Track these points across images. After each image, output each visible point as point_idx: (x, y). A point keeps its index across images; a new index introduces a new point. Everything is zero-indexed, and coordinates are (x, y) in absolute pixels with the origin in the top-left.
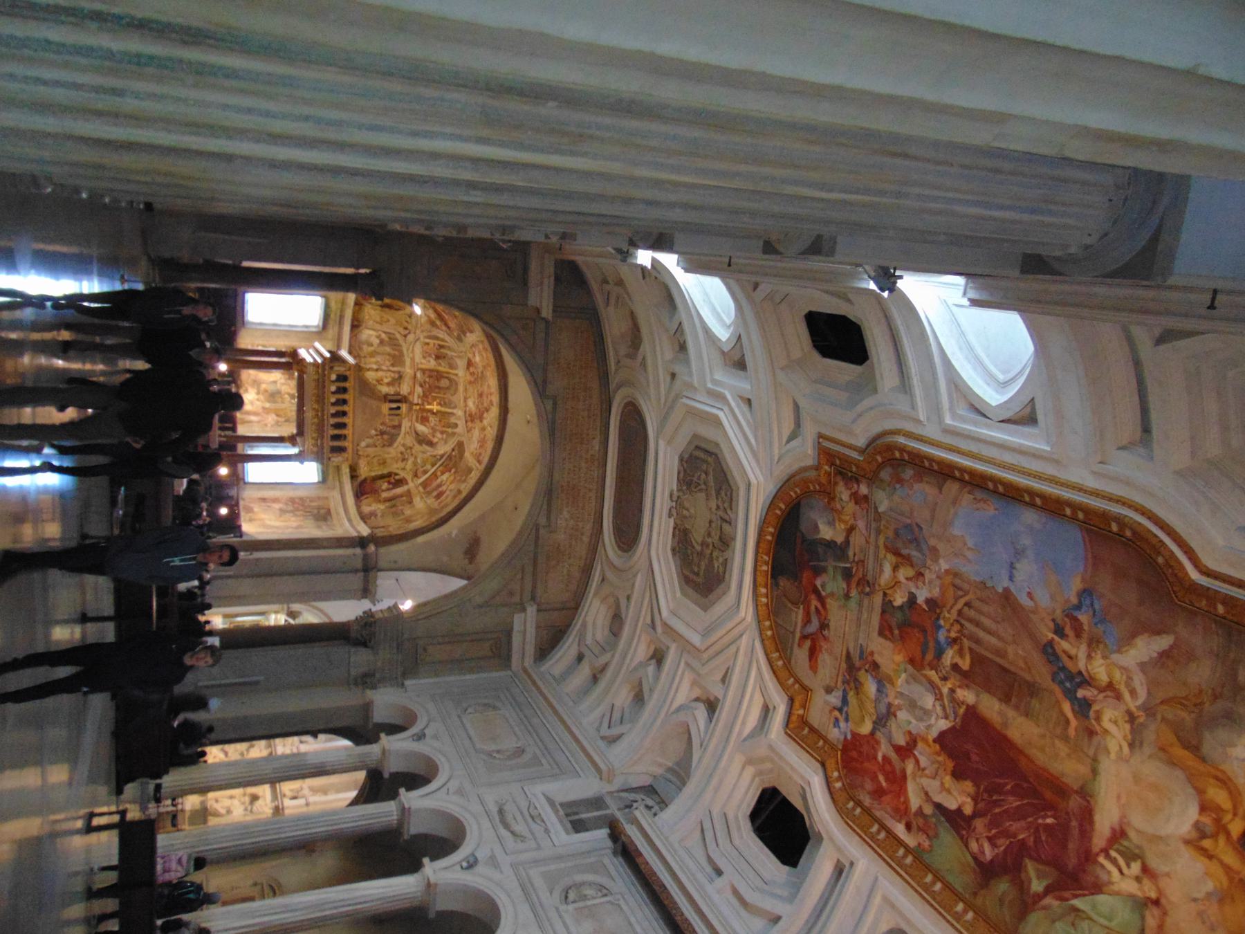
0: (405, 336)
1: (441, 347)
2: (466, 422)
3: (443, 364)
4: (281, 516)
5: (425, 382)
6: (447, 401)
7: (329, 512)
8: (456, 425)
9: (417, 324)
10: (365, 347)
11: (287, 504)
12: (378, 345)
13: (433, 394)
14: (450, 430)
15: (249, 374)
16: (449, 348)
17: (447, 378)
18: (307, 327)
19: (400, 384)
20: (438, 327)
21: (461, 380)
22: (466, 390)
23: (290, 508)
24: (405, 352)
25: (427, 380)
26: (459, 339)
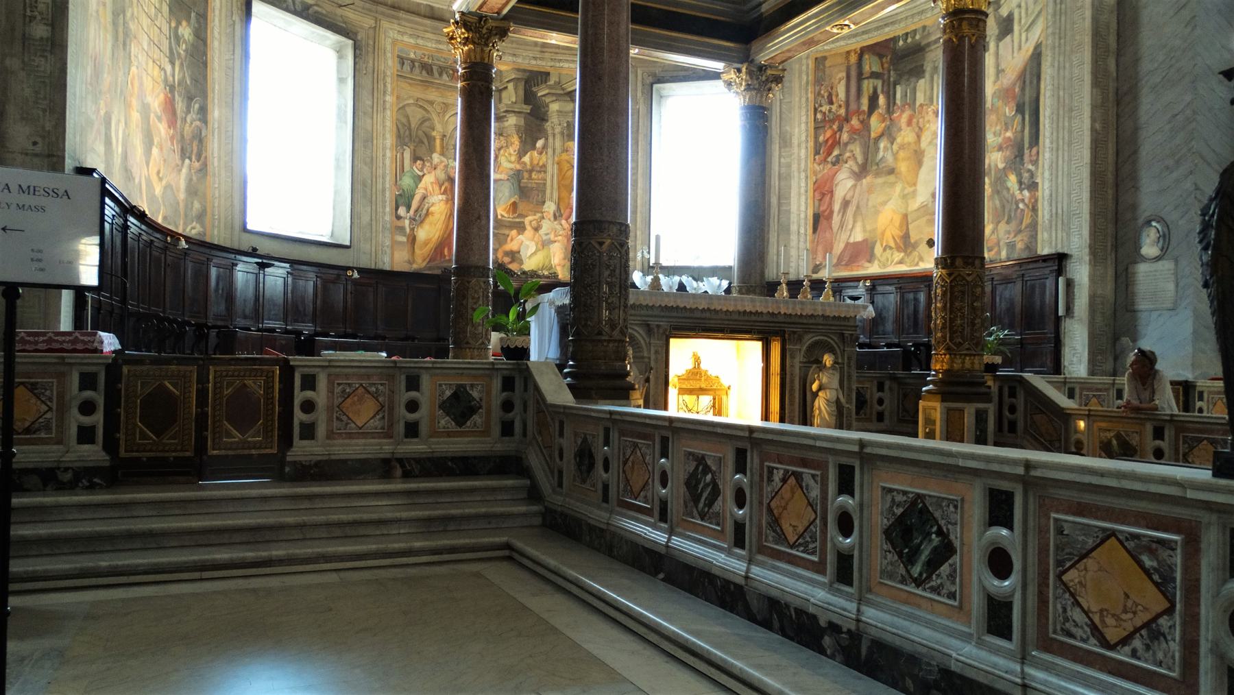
4: (892, 171)
7: (878, 49)
11: (834, 164)
18: (341, 80)
23: (857, 149)
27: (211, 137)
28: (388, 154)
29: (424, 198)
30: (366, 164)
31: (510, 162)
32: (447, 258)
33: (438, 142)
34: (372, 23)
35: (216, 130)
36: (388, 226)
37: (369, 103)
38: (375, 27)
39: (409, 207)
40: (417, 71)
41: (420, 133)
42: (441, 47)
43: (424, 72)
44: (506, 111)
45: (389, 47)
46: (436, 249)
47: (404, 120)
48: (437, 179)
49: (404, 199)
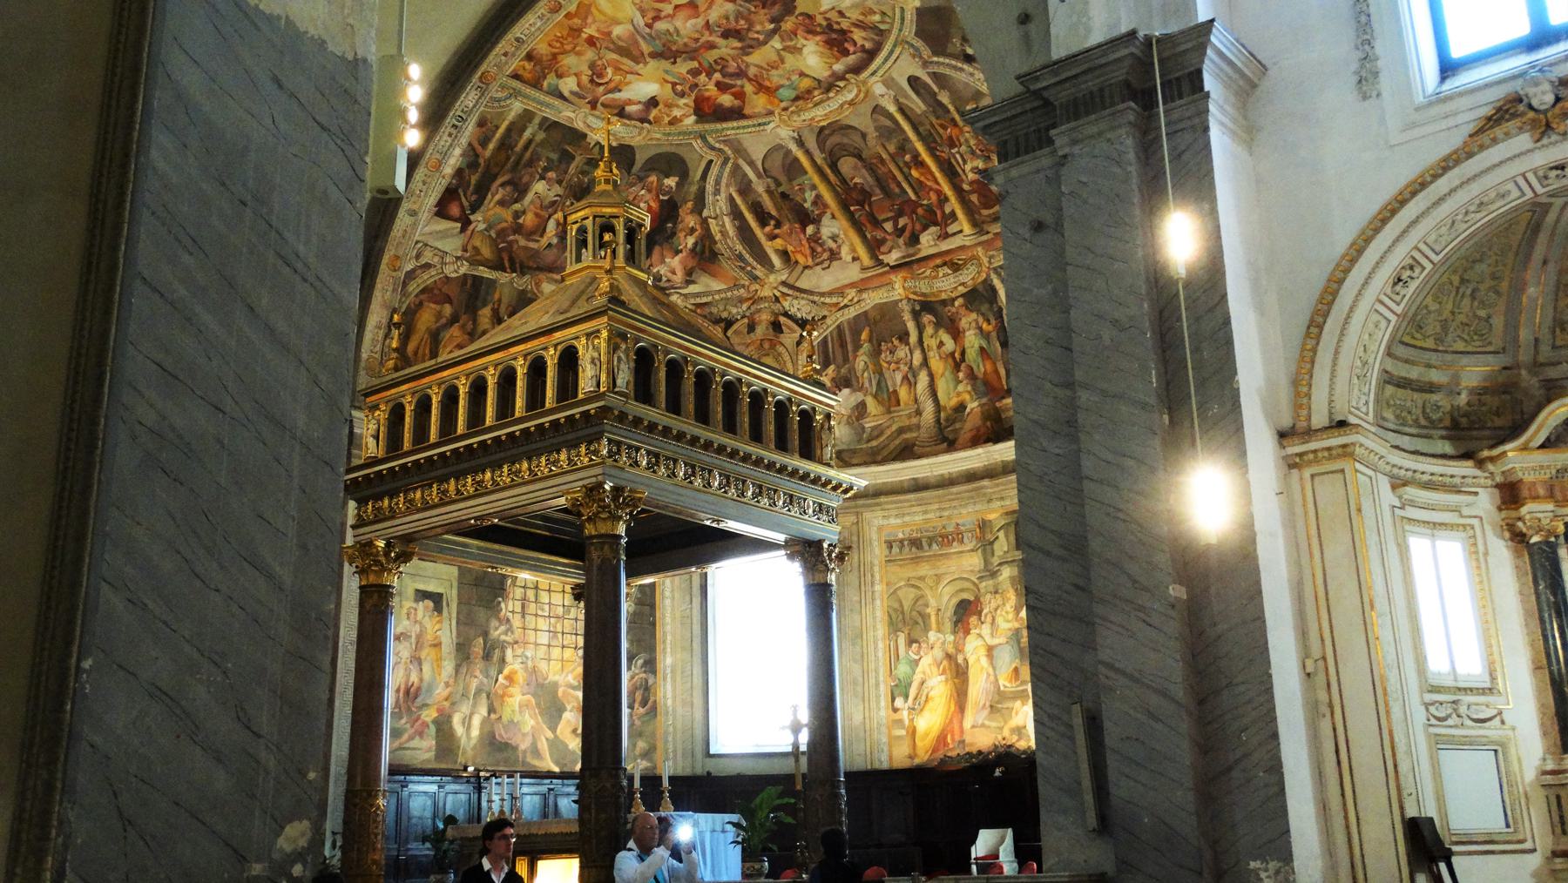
0: (802, 324)
1: (763, 218)
2: (871, 54)
3: (810, 196)
5: (899, 232)
6: (892, 148)
8: (913, 81)
9: (741, 301)
10: (869, 424)
12: (861, 389)
13: (913, 197)
14: (944, 98)
15: (973, 727)
16: (745, 189)
17: (834, 166)
19: (944, 303)
20: (707, 235)
21: (798, 121)
22: (802, 97)
24: (851, 313)
25: (888, 226)
26: (671, 163)
27: (662, 683)
28: (881, 645)
29: (922, 683)
30: (855, 661)
31: (1008, 621)
32: (951, 746)
33: (933, 618)
34: (853, 519)
35: (669, 676)
36: (884, 721)
37: (856, 598)
38: (858, 522)
39: (906, 697)
40: (907, 549)
41: (914, 613)
42: (929, 516)
43: (914, 549)
44: (1000, 564)
45: (875, 536)
46: (938, 737)
47: (896, 605)
48: (935, 660)
49: (900, 689)
